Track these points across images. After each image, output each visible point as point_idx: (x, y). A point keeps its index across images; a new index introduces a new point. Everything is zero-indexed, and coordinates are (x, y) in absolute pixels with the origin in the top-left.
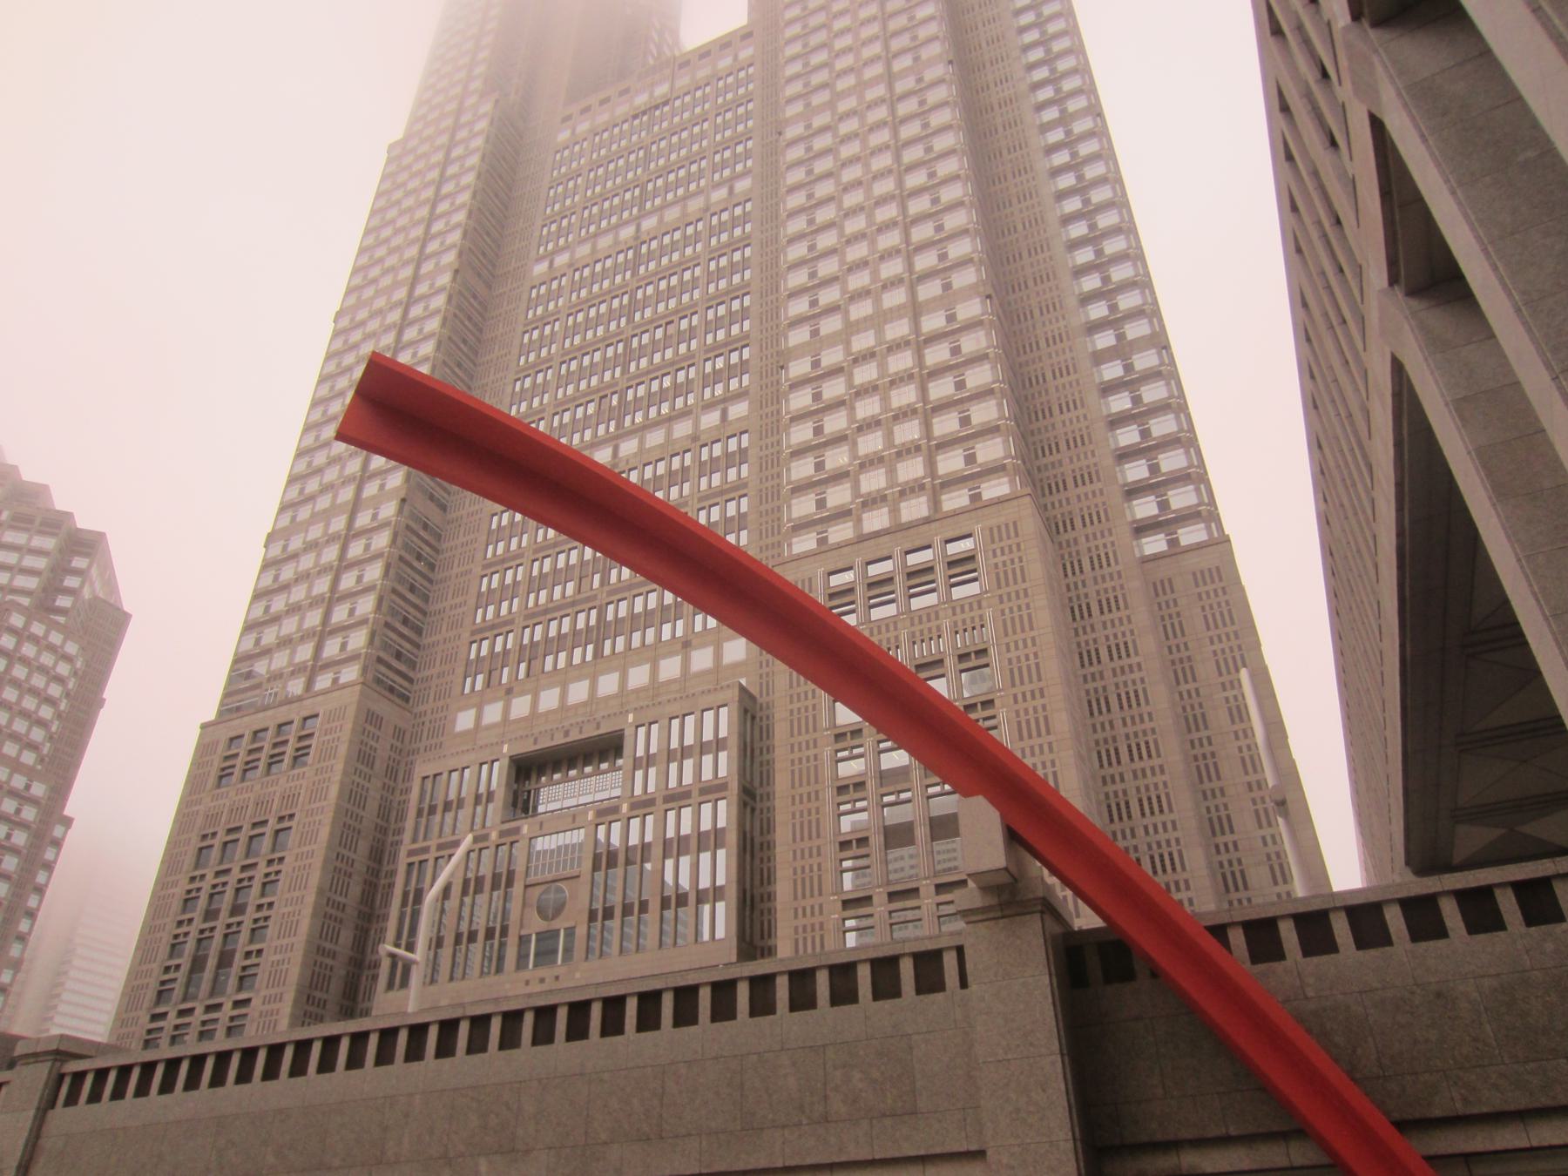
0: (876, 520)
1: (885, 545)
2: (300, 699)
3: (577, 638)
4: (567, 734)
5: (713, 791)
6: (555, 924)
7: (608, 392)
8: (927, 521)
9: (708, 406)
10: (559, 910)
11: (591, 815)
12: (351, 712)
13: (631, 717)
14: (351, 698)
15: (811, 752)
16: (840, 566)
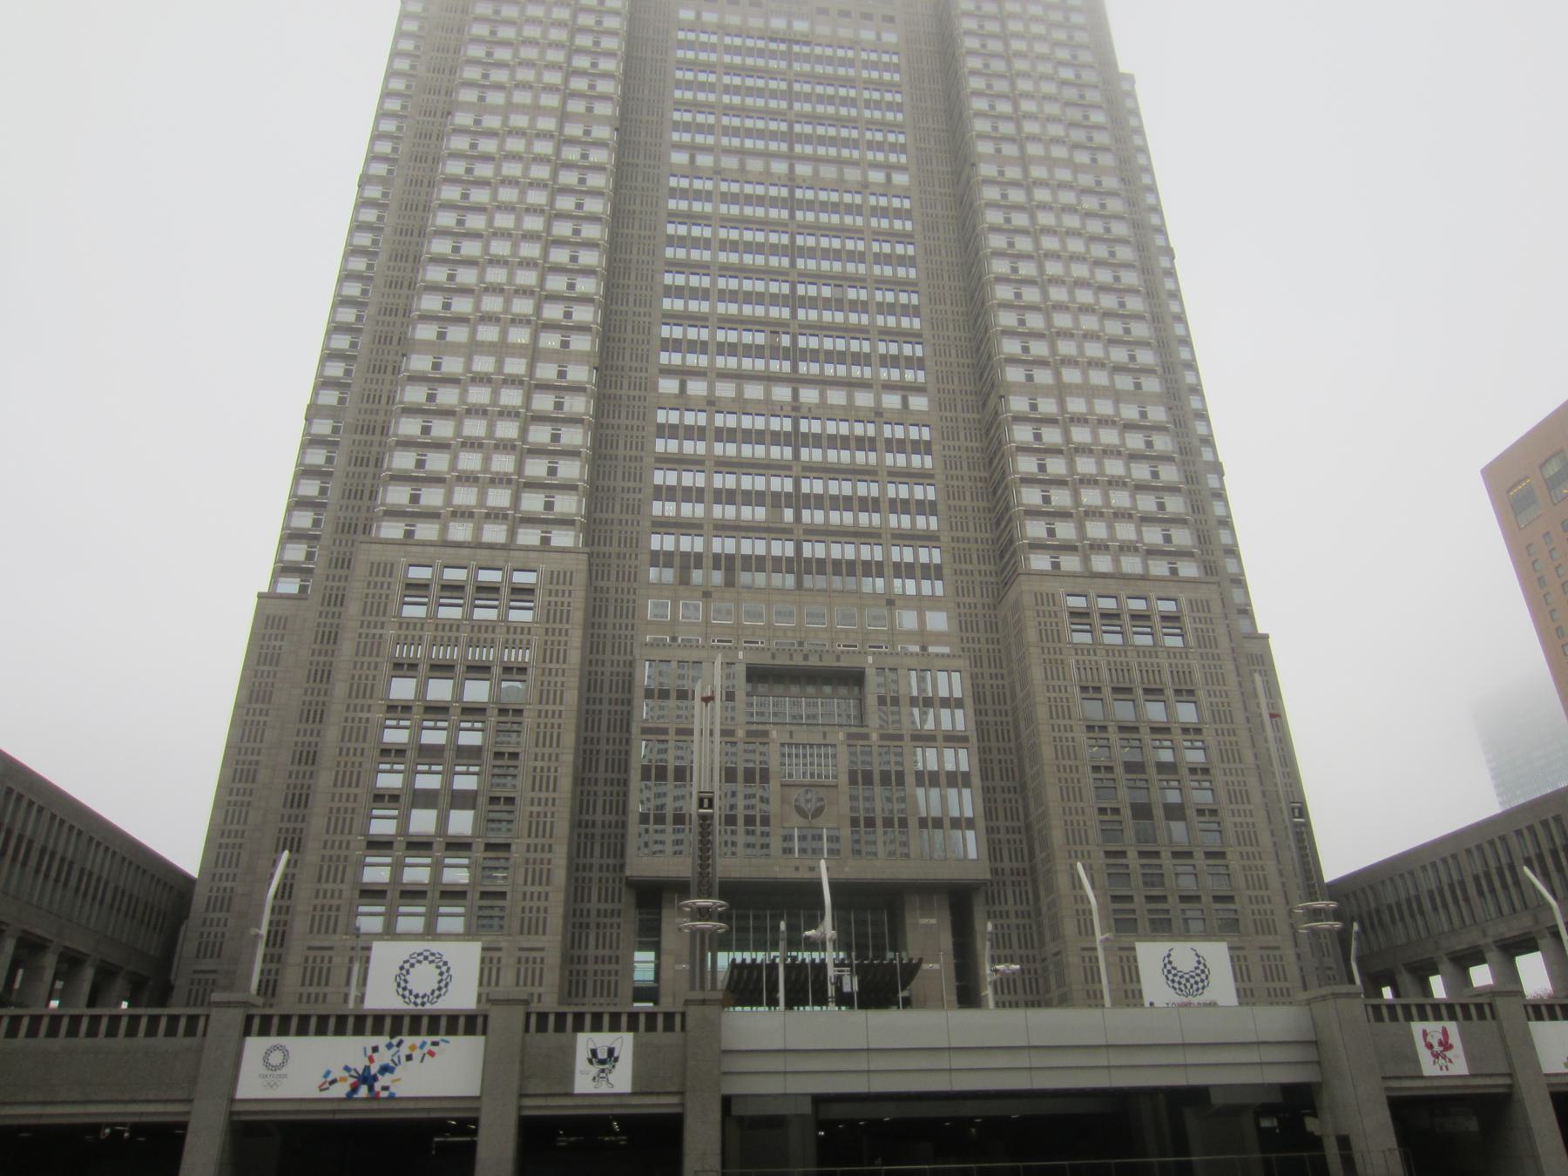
0: (1102, 563)
1: (1112, 586)
2: (503, 547)
3: (778, 564)
4: (806, 657)
5: (954, 739)
6: (817, 822)
7: (781, 330)
8: (1144, 577)
9: (889, 387)
10: (818, 812)
11: (841, 736)
12: (581, 579)
13: (870, 659)
14: (579, 565)
15: (1069, 735)
16: (1077, 591)
